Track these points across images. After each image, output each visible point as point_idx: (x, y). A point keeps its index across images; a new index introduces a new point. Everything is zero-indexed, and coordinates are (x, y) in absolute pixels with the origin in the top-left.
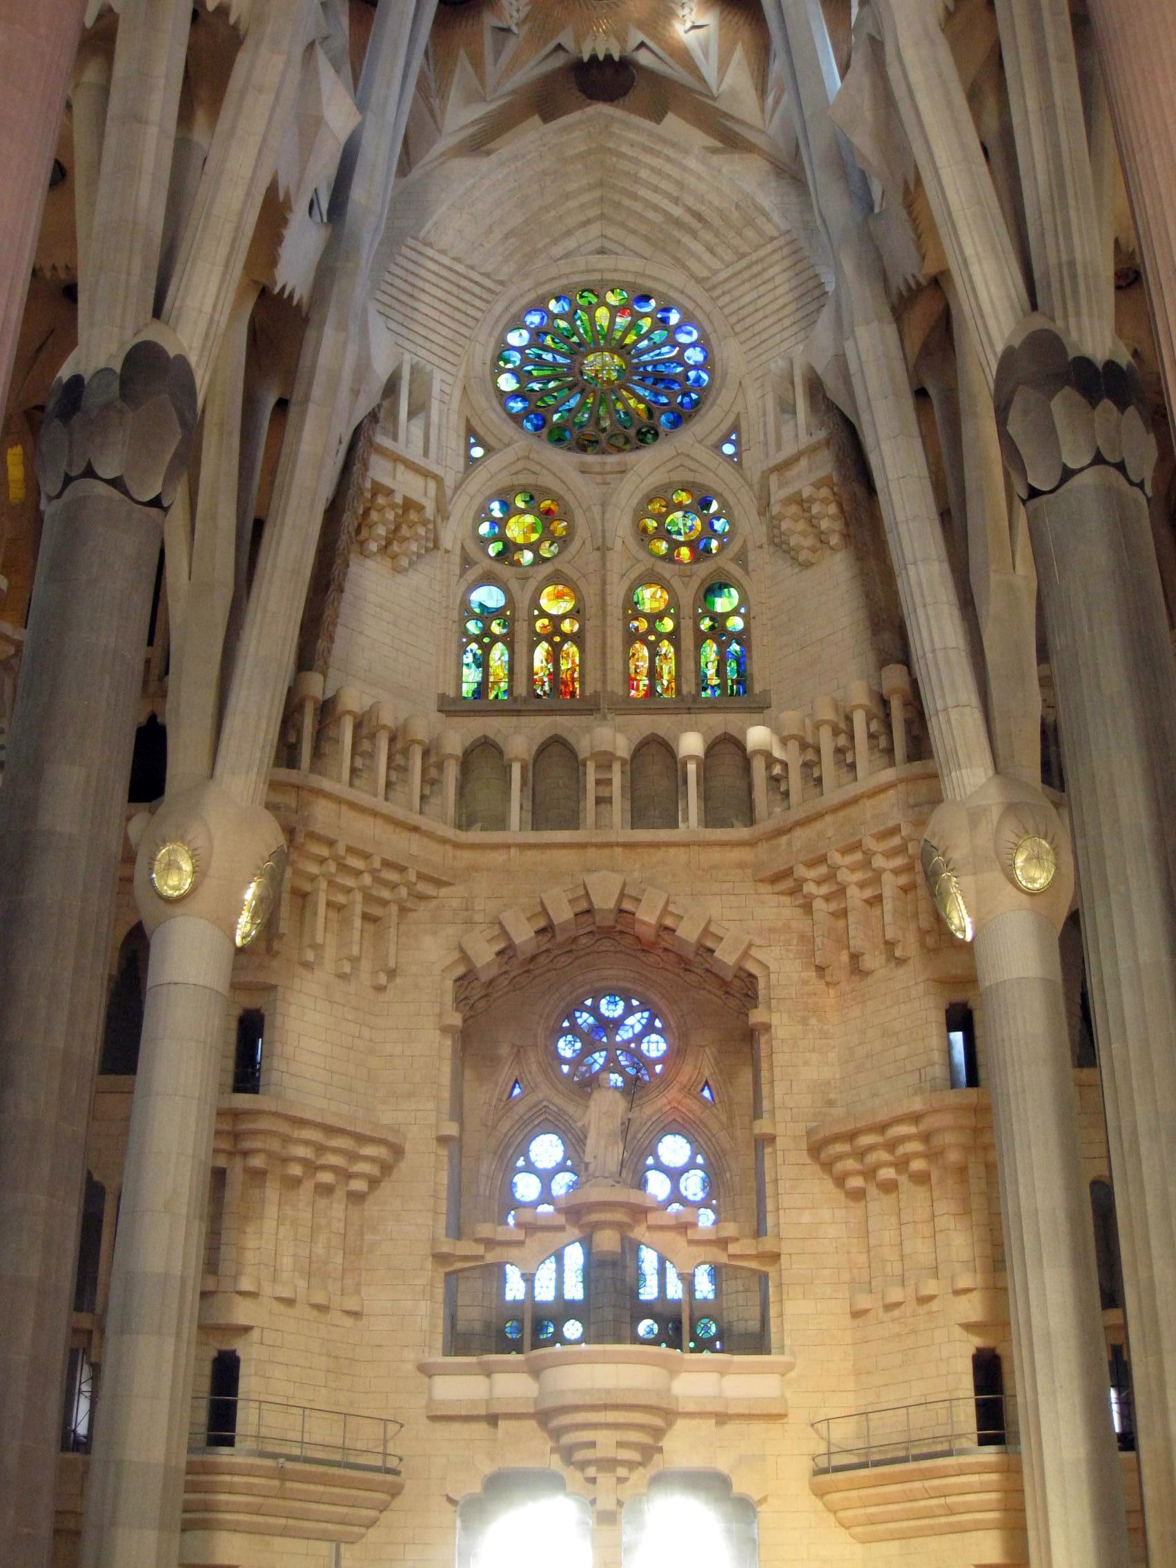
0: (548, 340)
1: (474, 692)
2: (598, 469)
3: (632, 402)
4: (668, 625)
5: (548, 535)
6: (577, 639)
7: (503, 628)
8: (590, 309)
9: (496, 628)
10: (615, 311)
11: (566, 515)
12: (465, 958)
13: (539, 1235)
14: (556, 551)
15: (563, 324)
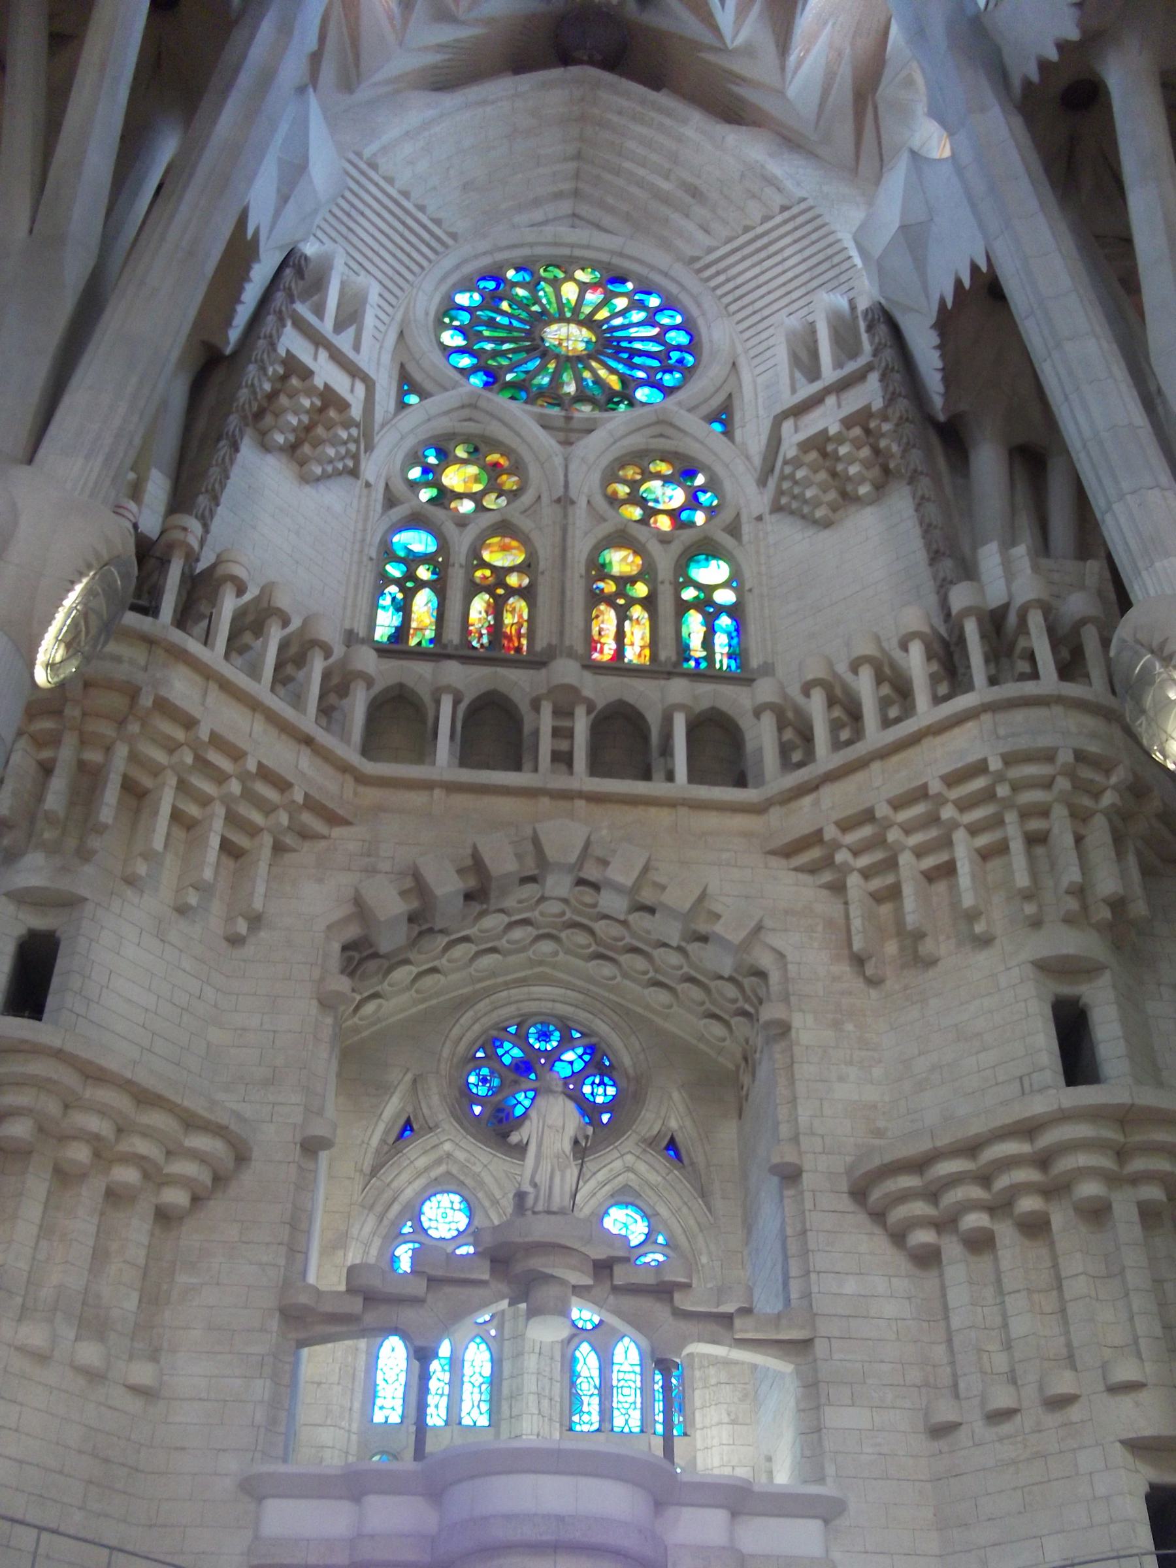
0: (505, 305)
1: (390, 637)
2: (560, 423)
3: (603, 373)
4: (641, 590)
5: (493, 486)
6: (525, 593)
7: (433, 573)
8: (556, 284)
9: (424, 573)
10: (584, 287)
11: (517, 468)
12: (360, 909)
13: (449, 1289)
14: (505, 503)
15: (521, 292)
